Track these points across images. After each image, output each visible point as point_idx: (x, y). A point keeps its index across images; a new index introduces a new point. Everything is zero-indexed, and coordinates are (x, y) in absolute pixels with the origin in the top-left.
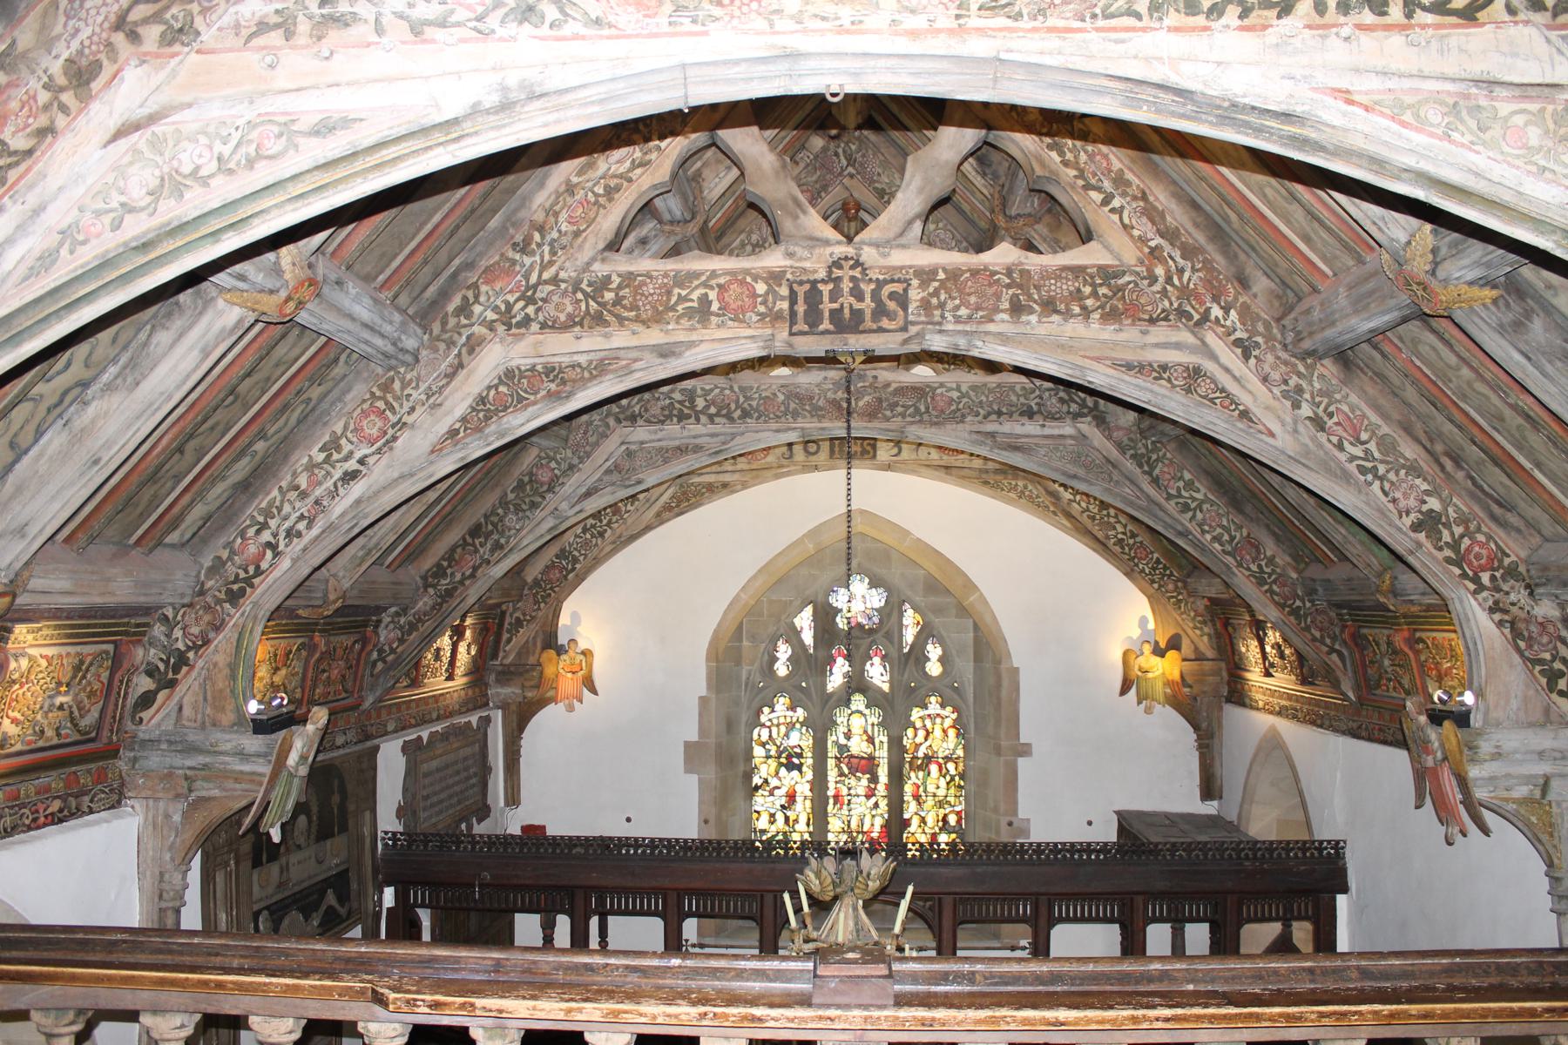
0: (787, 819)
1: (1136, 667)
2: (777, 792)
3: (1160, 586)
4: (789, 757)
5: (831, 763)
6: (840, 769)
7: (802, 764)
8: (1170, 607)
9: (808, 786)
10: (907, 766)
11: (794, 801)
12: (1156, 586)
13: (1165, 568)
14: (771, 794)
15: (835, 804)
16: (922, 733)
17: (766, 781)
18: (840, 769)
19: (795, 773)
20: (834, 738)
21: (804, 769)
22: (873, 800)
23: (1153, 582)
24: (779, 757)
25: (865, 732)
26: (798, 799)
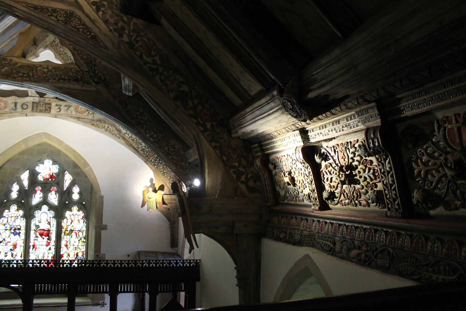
0: (12, 254)
1: (147, 197)
2: (9, 244)
3: (157, 167)
4: (15, 229)
5: (32, 232)
6: (36, 234)
7: (20, 233)
8: (160, 175)
9: (22, 241)
10: (63, 234)
11: (16, 247)
12: (156, 167)
13: (159, 160)
14: (6, 245)
15: (33, 248)
16: (70, 221)
17: (4, 240)
18: (36, 234)
19: (17, 236)
20: (34, 222)
21: (21, 234)
22: (49, 247)
23: (155, 165)
24: (11, 230)
25: (47, 220)
26: (17, 246)
